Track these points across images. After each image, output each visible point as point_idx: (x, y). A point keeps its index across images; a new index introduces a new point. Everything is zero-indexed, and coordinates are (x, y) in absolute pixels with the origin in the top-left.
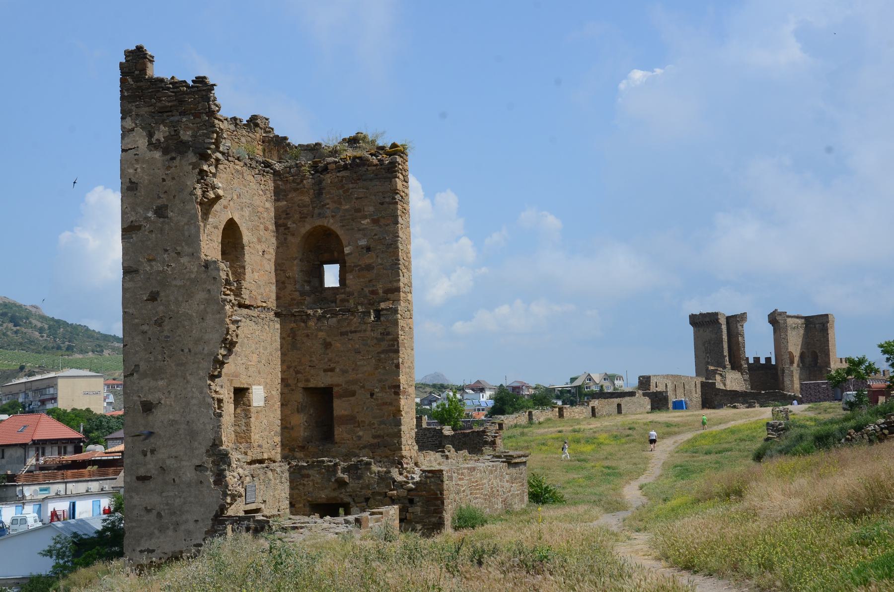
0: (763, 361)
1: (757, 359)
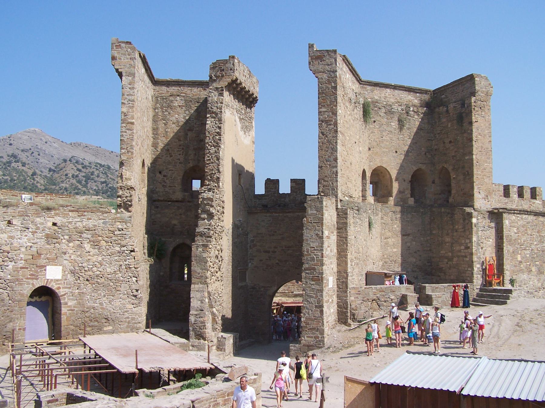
1: (298, 185)
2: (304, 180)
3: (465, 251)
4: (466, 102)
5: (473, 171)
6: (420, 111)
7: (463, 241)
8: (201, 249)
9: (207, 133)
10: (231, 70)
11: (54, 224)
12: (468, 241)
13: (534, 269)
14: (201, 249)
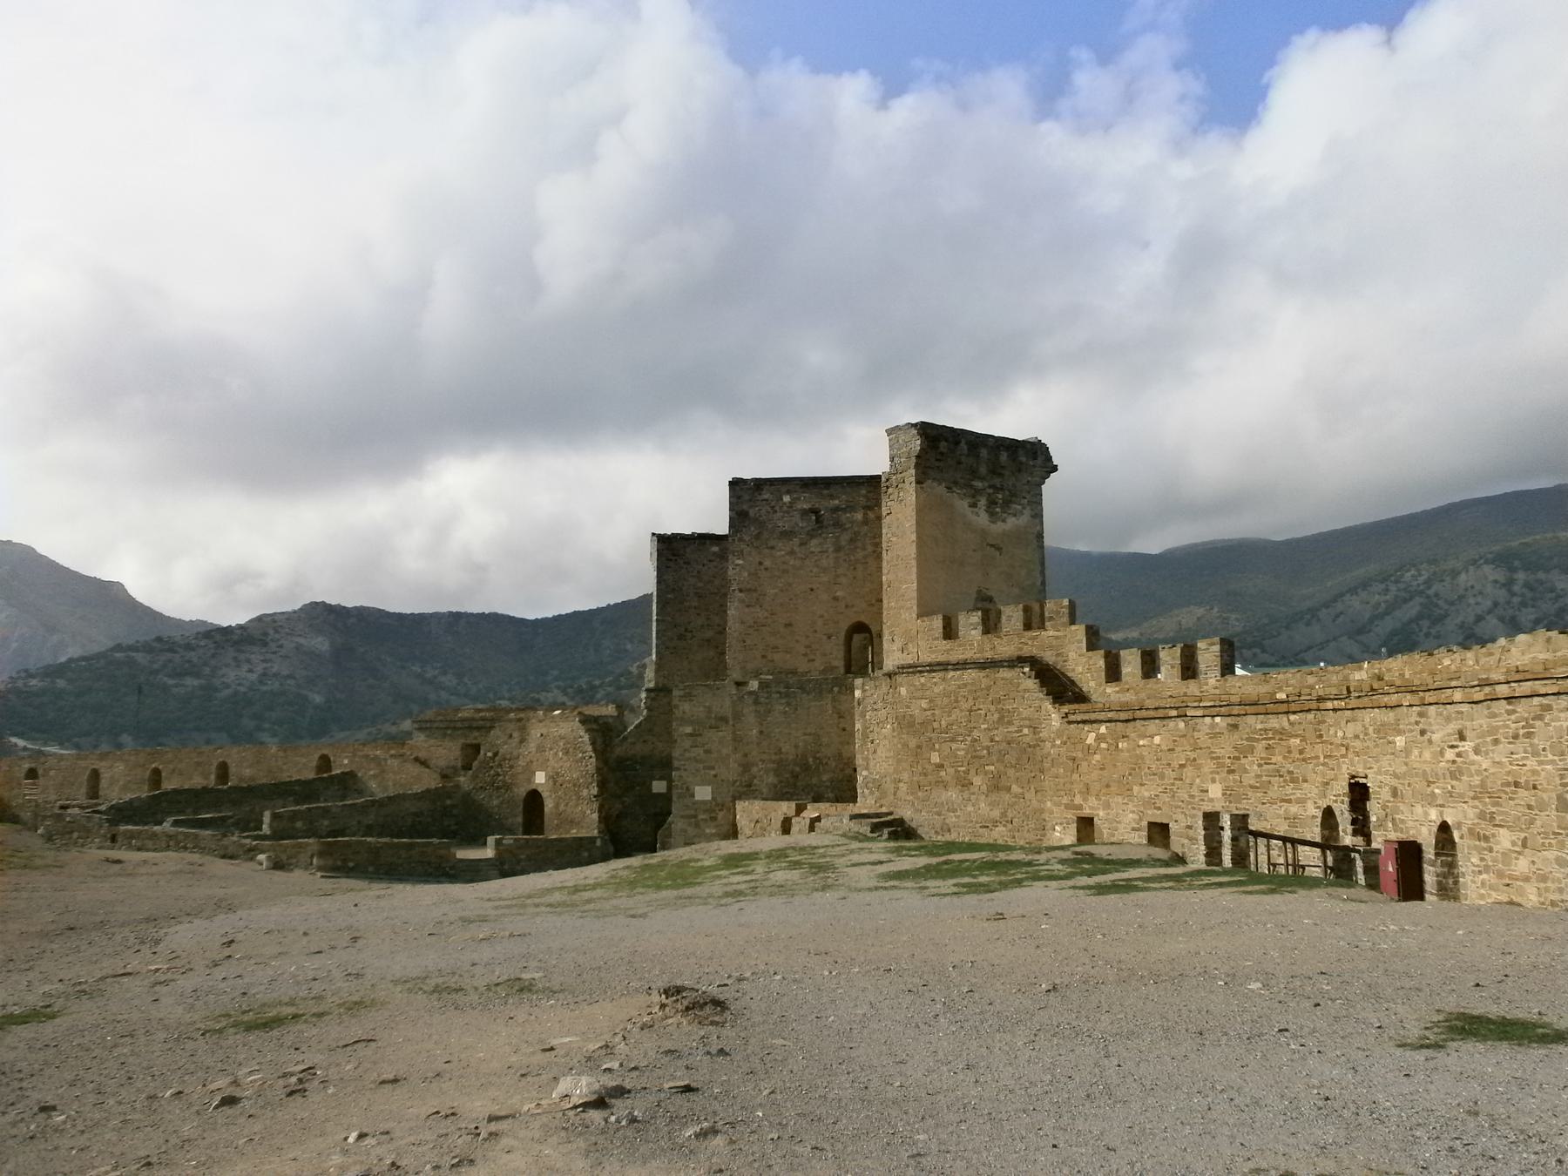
13: (977, 780)
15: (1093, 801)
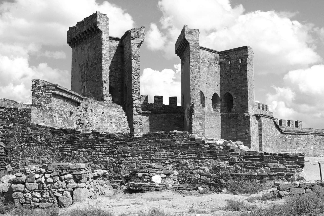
0: (166, 102)
2: (162, 97)
3: (245, 135)
4: (243, 60)
5: (247, 95)
6: (215, 62)
7: (244, 130)
8: (139, 131)
9: (133, 69)
10: (143, 34)
11: (103, 113)
12: (247, 130)
13: (270, 145)
14: (139, 131)
15: (288, 150)
